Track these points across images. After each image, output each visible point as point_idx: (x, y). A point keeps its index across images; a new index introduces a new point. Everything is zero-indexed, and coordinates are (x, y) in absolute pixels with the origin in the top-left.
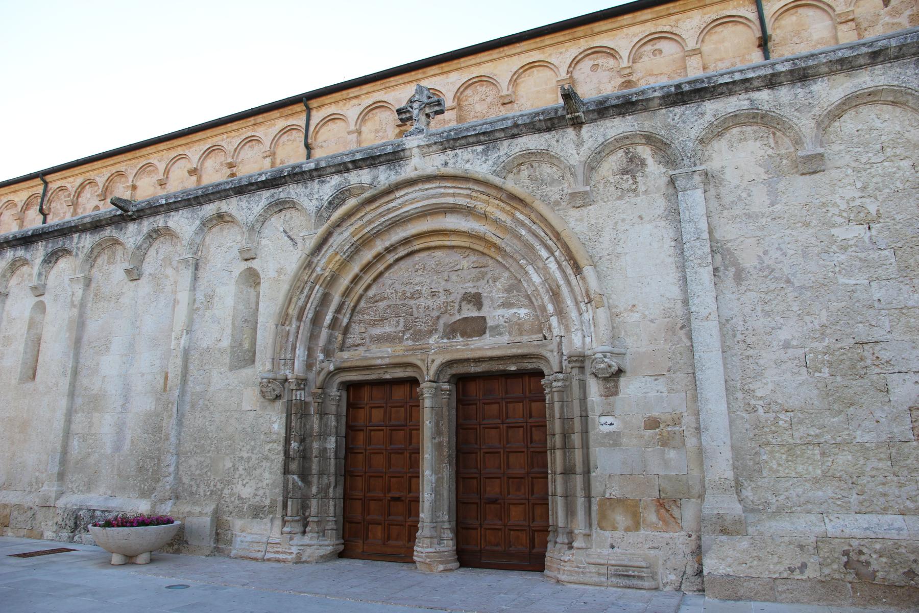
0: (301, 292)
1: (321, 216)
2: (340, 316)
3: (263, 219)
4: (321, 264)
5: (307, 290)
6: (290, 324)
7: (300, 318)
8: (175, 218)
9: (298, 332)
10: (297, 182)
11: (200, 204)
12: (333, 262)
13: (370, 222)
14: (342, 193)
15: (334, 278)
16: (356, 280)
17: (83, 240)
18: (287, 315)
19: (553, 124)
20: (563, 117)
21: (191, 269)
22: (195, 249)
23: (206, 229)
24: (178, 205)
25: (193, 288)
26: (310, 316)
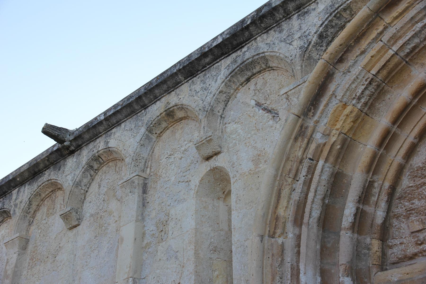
0: (295, 178)
1: (310, 58)
2: (369, 209)
3: (226, 97)
4: (321, 127)
5: (304, 172)
6: (284, 233)
7: (298, 221)
8: (118, 134)
9: (298, 246)
10: (267, 30)
11: (145, 107)
12: (343, 118)
13: (394, 38)
14: (338, 16)
15: (346, 148)
16: (387, 140)
17: (21, 194)
18: (277, 219)
21: (138, 191)
22: (142, 165)
23: (154, 137)
24: (119, 116)
25: (141, 217)
26: (316, 214)
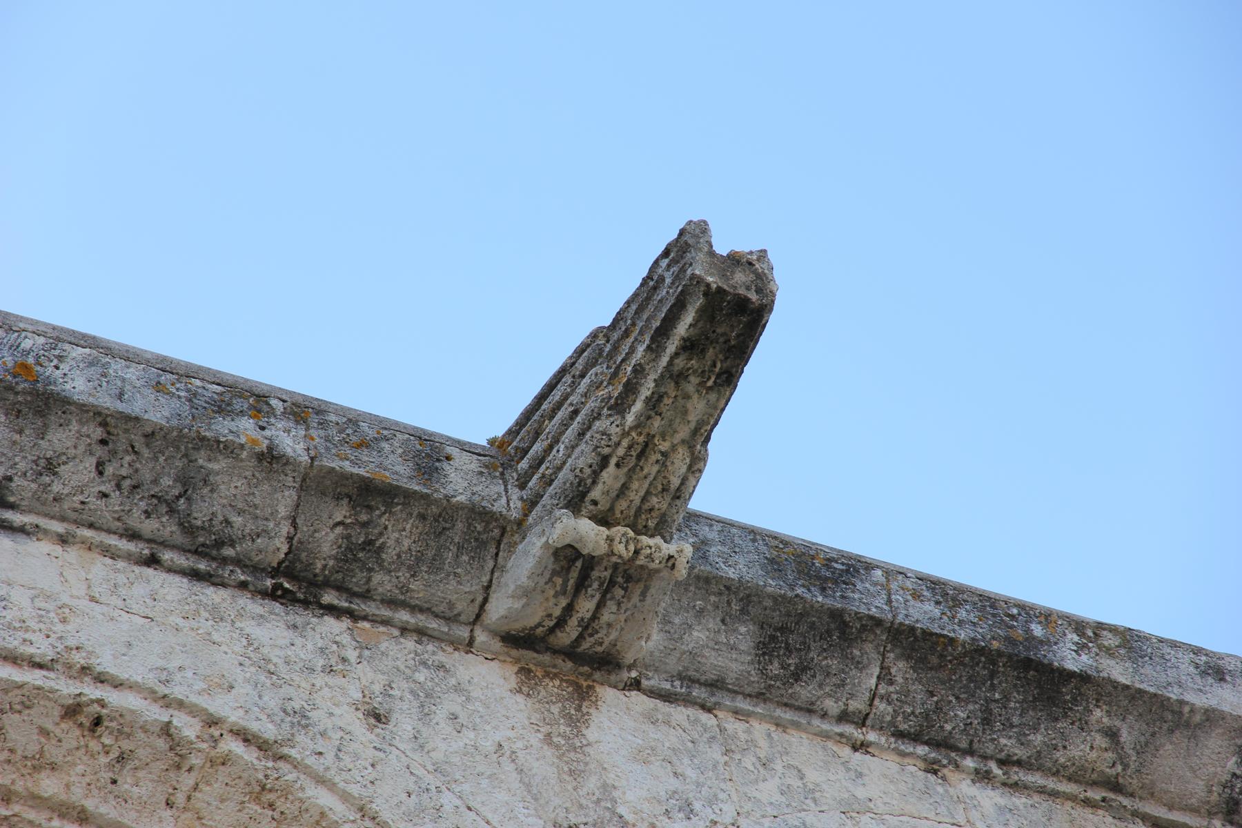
19: (361, 550)
20: (490, 534)
